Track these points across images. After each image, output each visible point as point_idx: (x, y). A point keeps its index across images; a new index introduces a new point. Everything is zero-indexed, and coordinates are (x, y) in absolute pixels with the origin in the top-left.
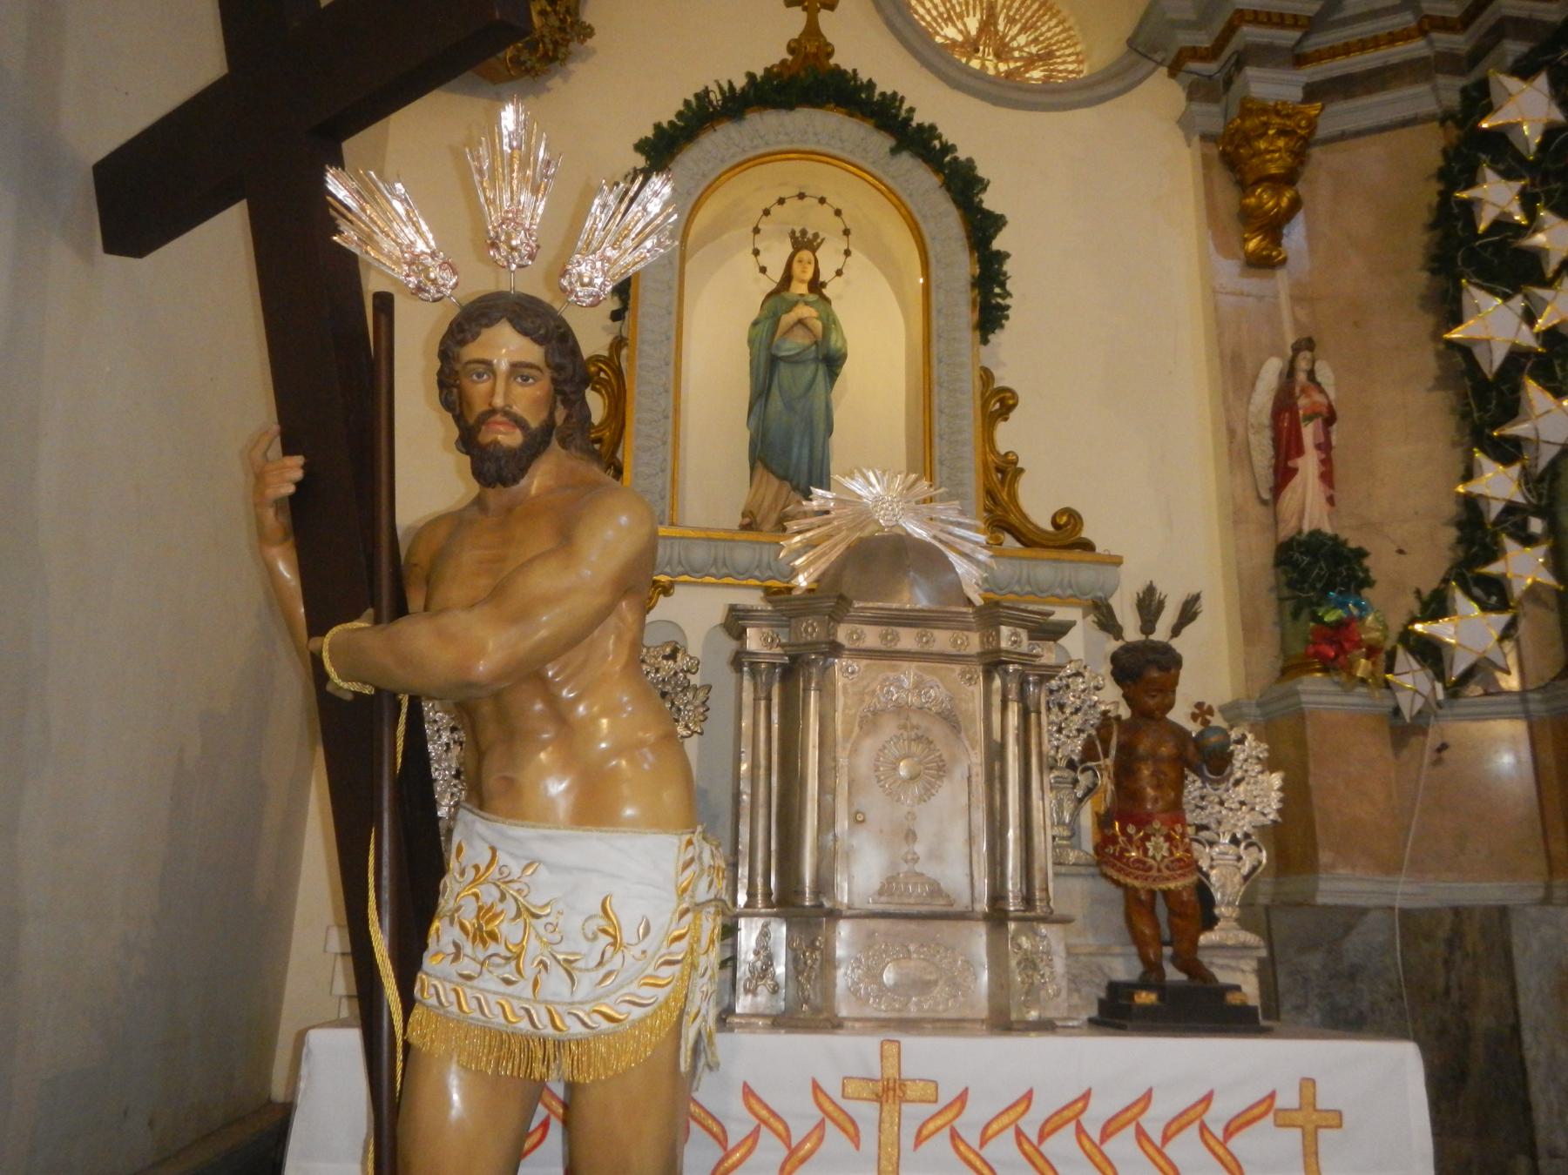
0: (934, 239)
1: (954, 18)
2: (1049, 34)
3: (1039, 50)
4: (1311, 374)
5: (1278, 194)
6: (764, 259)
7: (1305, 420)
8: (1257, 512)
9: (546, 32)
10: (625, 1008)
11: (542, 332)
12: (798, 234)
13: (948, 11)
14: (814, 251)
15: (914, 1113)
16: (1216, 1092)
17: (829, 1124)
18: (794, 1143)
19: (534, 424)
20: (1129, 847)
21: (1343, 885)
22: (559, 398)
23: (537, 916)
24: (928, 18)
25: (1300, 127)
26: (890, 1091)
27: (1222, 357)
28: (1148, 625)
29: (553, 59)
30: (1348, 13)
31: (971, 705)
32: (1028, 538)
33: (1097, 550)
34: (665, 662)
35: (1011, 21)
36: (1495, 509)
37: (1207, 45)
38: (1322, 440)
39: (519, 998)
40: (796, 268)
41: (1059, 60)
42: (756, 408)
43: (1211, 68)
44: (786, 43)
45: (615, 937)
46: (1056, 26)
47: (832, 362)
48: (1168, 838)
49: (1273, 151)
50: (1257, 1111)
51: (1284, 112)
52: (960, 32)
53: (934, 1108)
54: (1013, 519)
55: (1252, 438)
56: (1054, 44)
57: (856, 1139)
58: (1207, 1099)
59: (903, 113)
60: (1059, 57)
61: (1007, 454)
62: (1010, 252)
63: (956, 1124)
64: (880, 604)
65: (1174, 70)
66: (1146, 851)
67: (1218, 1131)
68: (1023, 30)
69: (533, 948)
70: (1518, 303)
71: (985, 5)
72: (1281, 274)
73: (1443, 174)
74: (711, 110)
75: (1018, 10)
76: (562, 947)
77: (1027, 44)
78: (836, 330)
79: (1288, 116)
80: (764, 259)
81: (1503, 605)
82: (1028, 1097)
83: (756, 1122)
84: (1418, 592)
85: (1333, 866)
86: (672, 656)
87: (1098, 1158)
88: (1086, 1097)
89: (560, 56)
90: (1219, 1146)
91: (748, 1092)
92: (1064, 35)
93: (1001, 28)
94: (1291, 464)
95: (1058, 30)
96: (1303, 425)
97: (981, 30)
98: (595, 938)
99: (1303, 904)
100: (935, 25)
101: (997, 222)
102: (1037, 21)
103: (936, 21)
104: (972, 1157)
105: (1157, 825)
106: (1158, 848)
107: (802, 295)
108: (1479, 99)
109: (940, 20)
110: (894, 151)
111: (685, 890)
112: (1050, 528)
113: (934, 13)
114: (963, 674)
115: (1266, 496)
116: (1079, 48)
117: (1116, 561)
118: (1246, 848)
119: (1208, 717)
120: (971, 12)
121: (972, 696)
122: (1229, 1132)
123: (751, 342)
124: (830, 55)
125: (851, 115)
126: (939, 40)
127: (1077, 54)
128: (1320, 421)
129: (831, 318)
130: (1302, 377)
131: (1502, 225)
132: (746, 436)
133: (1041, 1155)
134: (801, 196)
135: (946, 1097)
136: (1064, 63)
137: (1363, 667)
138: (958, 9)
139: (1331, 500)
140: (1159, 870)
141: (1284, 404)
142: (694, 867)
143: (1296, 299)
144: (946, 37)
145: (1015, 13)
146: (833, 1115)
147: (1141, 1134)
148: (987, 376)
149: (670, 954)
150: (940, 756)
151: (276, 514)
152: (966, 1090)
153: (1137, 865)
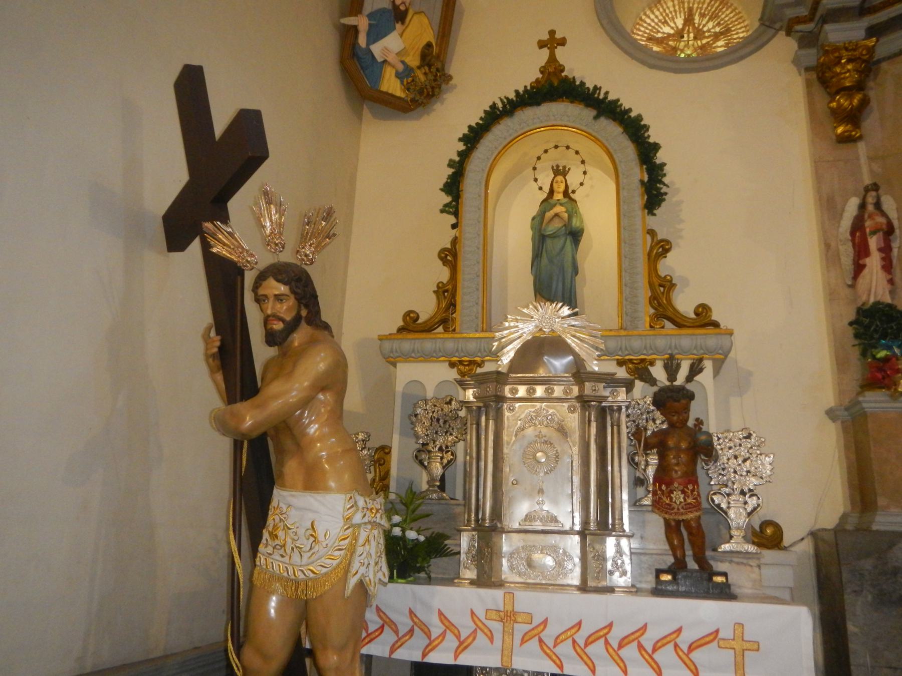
0: (621, 162)
1: (669, 21)
2: (727, 19)
3: (721, 29)
4: (878, 205)
5: (850, 97)
7: (870, 234)
8: (845, 292)
9: (427, 83)
10: (320, 568)
11: (286, 280)
12: (555, 168)
13: (664, 18)
14: (564, 176)
15: (520, 629)
16: (683, 627)
17: (479, 631)
18: (462, 639)
19: (288, 318)
20: (662, 497)
22: (302, 306)
23: (289, 529)
24: (653, 24)
25: (863, 55)
26: (508, 617)
27: (820, 199)
28: (672, 376)
29: (433, 95)
31: (573, 424)
32: (679, 322)
33: (721, 327)
34: (445, 406)
35: (702, 16)
37: (806, 14)
38: (883, 245)
39: (285, 563)
40: (555, 185)
41: (734, 33)
42: (535, 263)
43: (810, 26)
44: (538, 70)
45: (315, 538)
46: (731, 12)
47: (575, 235)
48: (683, 492)
49: (845, 73)
50: (707, 639)
51: (851, 48)
52: (672, 28)
53: (531, 627)
54: (669, 314)
55: (841, 247)
56: (730, 24)
57: (491, 640)
58: (679, 630)
59: (601, 96)
60: (734, 31)
61: (665, 277)
62: (665, 162)
63: (542, 635)
64: (531, 375)
65: (789, 33)
66: (671, 499)
67: (685, 648)
68: (711, 19)
69: (289, 541)
71: (686, 10)
72: (861, 147)
74: (498, 113)
75: (707, 8)
76: (298, 542)
77: (714, 27)
79: (854, 50)
82: (579, 624)
83: (444, 628)
86: (450, 403)
87: (616, 658)
88: (610, 625)
89: (436, 93)
90: (686, 656)
91: (440, 613)
92: (736, 17)
93: (697, 21)
94: (861, 262)
95: (732, 15)
97: (684, 25)
98: (308, 539)
99: (868, 530)
100: (657, 27)
101: (656, 147)
102: (718, 13)
103: (657, 24)
104: (548, 651)
105: (676, 485)
106: (678, 497)
107: (558, 200)
109: (660, 24)
110: (596, 118)
111: (348, 518)
112: (693, 316)
113: (656, 20)
114: (569, 407)
116: (746, 23)
118: (750, 497)
119: (701, 426)
120: (678, 16)
121: (573, 420)
122: (691, 648)
123: (532, 228)
125: (572, 102)
126: (660, 35)
127: (745, 27)
128: (881, 233)
129: (574, 210)
130: (870, 208)
132: (530, 279)
133: (585, 653)
134: (556, 147)
135: (536, 622)
136: (737, 33)
138: (670, 16)
139: (891, 282)
140: (678, 509)
141: (858, 226)
142: (354, 508)
143: (871, 159)
144: (664, 33)
145: (705, 11)
146: (479, 627)
147: (641, 647)
148: (652, 233)
149: (339, 546)
150: (557, 450)
151: (214, 360)
152: (547, 618)
153: (666, 506)
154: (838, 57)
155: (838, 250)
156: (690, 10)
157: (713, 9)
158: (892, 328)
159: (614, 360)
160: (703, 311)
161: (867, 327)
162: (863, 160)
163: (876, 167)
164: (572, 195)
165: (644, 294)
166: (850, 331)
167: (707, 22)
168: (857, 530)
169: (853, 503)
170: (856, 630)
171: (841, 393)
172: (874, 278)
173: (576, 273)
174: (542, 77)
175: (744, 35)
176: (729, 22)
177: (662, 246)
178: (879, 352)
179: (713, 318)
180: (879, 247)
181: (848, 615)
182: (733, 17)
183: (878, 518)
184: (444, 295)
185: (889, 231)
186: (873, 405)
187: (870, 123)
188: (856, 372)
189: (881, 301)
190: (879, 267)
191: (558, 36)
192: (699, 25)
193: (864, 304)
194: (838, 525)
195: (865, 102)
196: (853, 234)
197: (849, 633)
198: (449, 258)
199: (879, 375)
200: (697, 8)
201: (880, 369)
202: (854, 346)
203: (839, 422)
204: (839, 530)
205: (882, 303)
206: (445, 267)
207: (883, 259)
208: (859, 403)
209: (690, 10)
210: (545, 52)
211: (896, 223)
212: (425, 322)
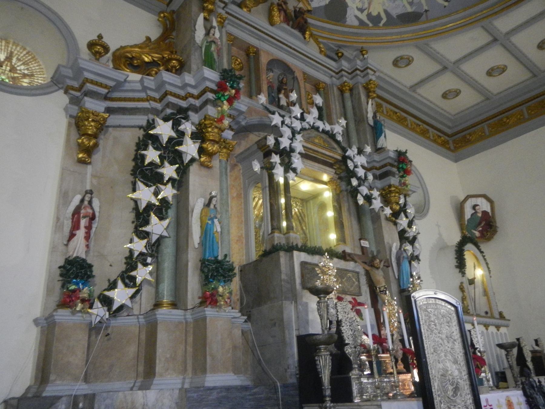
2: (33, 68)
4: (90, 202)
5: (90, 140)
8: (61, 248)
21: (60, 388)
27: (61, 191)
30: (125, 88)
35: (19, 60)
36: (136, 254)
37: (78, 86)
38: (87, 225)
41: (36, 78)
43: (78, 94)
51: (95, 114)
55: (65, 221)
60: (36, 77)
65: (66, 92)
68: (24, 64)
70: (153, 189)
71: (9, 52)
72: (89, 167)
73: (138, 145)
75: (22, 57)
77: (24, 70)
79: (97, 116)
81: (134, 285)
84: (109, 280)
85: (55, 380)
92: (40, 70)
94: (74, 232)
96: (81, 219)
108: (151, 125)
116: (44, 76)
127: (44, 78)
128: (88, 218)
130: (86, 203)
131: (151, 164)
136: (38, 79)
137: (79, 306)
139: (87, 246)
141: (77, 212)
143: (93, 176)
154: (87, 116)
156: (11, 53)
157: (26, 59)
158: (81, 272)
161: (68, 271)
162: (89, 176)
163: (95, 182)
166: (58, 272)
167: (21, 65)
168: (34, 397)
169: (36, 378)
171: (45, 308)
172: (79, 242)
175: (42, 82)
176: (34, 71)
178: (70, 287)
182: (38, 69)
183: (48, 389)
185: (93, 218)
186: (61, 317)
187: (97, 157)
188: (56, 297)
189: (80, 256)
192: (15, 64)
193: (69, 257)
195: (96, 145)
196: (73, 215)
199: (68, 300)
200: (16, 54)
201: (69, 296)
202: (58, 281)
205: (80, 258)
207: (86, 233)
208: (53, 316)
209: (11, 53)
211: (97, 214)
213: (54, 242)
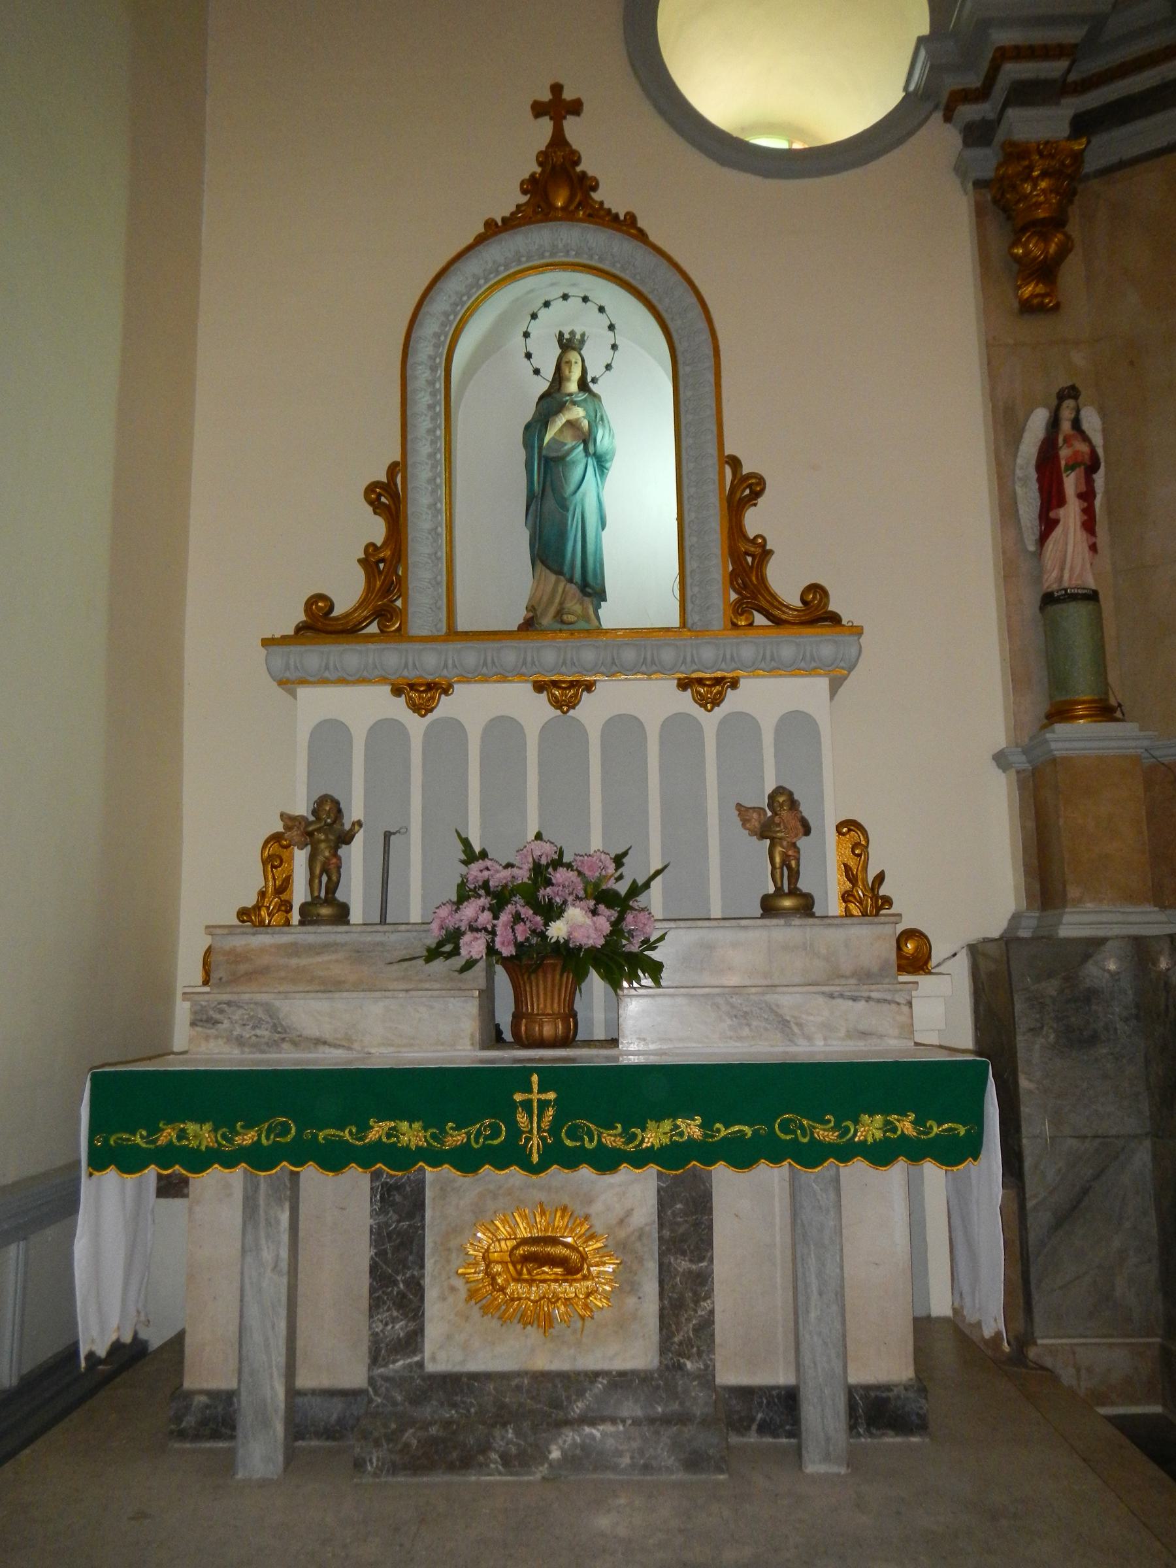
4: (1076, 424)
5: (1045, 238)
6: (536, 362)
7: (1066, 470)
33: (844, 622)
38: (1083, 488)
78: (604, 426)
80: (536, 362)
94: (1052, 515)
96: (1064, 475)
112: (799, 604)
115: (1032, 548)
117: (858, 631)
124: (577, 162)
128: (1080, 471)
130: (1066, 426)
155: (1014, 490)
159: (674, 679)
160: (815, 593)
164: (591, 385)
165: (717, 567)
169: (1030, 896)
170: (1032, 1086)
171: (1016, 725)
173: (603, 526)
174: (543, 171)
177: (750, 486)
179: (830, 608)
180: (1079, 491)
181: (1021, 1065)
183: (1066, 918)
184: (378, 567)
190: (1079, 524)
191: (568, 95)
194: (1006, 931)
197: (1021, 1091)
198: (383, 499)
203: (1013, 773)
204: (1008, 940)
206: (377, 517)
210: (546, 126)
211: (1100, 452)
212: (346, 616)
213: (1004, 553)
